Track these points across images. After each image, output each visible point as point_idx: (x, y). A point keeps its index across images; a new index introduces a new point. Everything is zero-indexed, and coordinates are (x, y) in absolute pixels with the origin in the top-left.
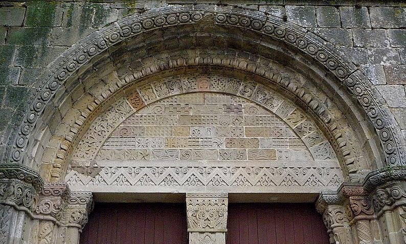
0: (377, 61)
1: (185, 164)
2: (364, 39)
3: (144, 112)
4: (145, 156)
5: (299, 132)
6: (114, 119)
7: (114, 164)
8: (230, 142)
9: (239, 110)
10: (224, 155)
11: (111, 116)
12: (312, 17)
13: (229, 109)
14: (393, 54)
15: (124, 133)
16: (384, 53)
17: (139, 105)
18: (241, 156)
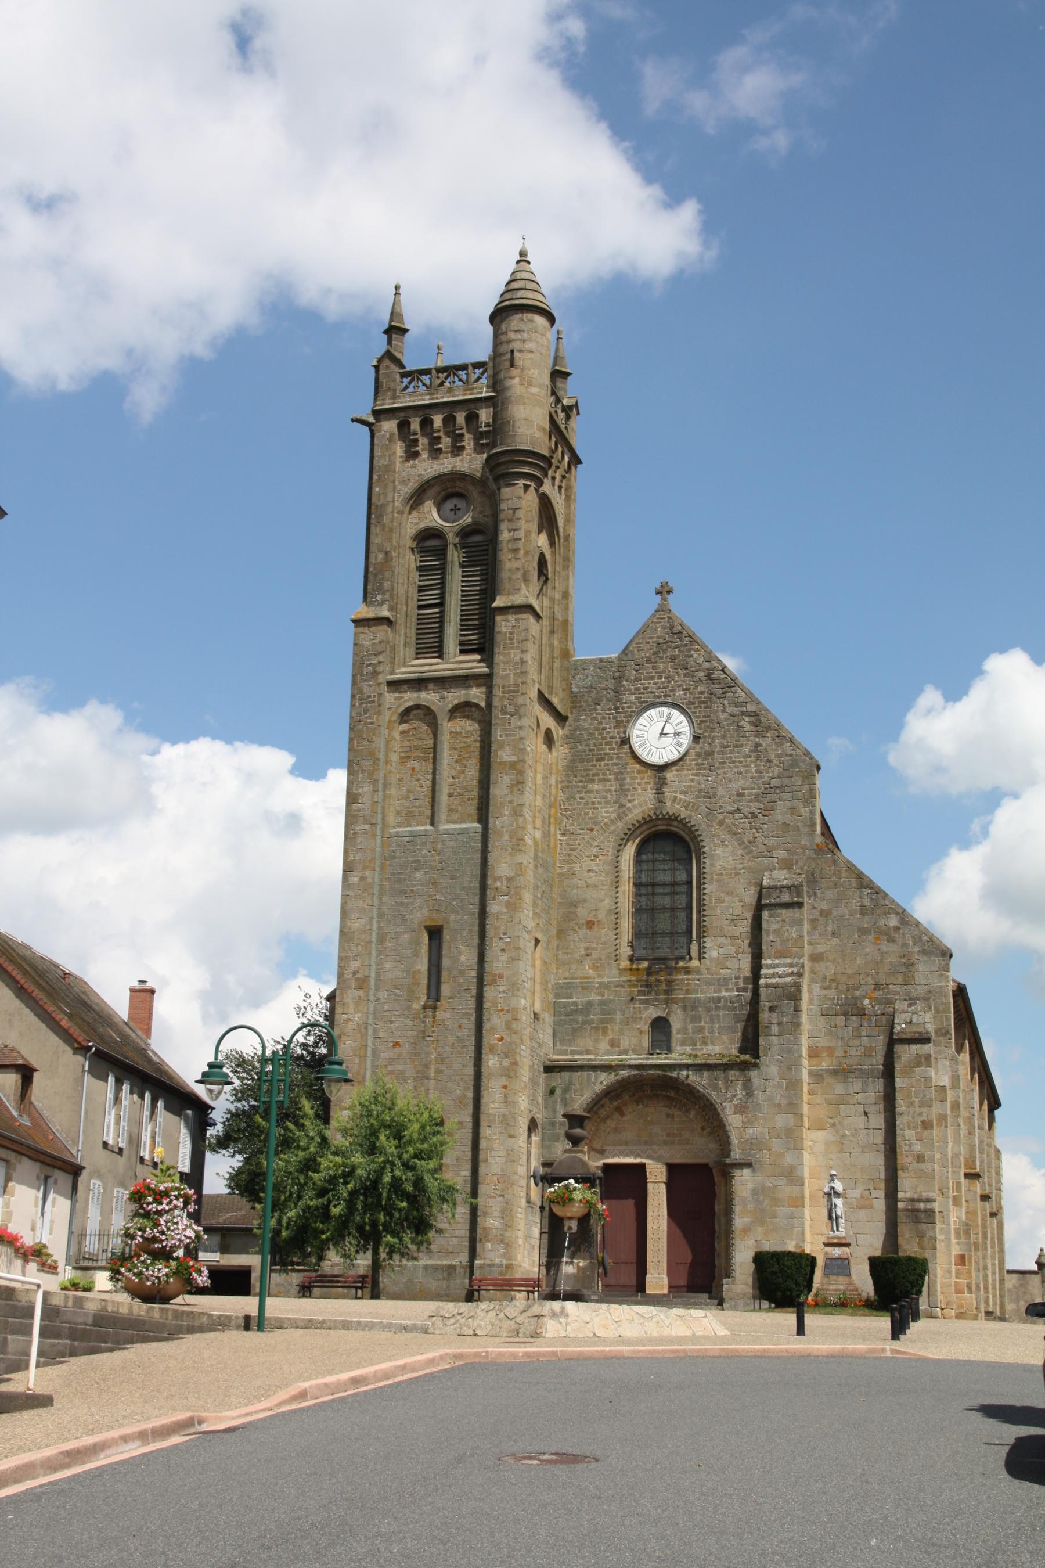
0: (731, 1101)
1: (646, 1148)
2: (727, 1088)
3: (625, 1118)
4: (626, 1143)
5: (703, 1129)
6: (611, 1123)
7: (611, 1148)
8: (668, 1135)
9: (673, 1116)
10: (665, 1143)
11: (608, 1122)
12: (702, 1077)
13: (668, 1115)
14: (740, 1096)
15: (616, 1130)
16: (735, 1096)
17: (622, 1114)
18: (673, 1143)
